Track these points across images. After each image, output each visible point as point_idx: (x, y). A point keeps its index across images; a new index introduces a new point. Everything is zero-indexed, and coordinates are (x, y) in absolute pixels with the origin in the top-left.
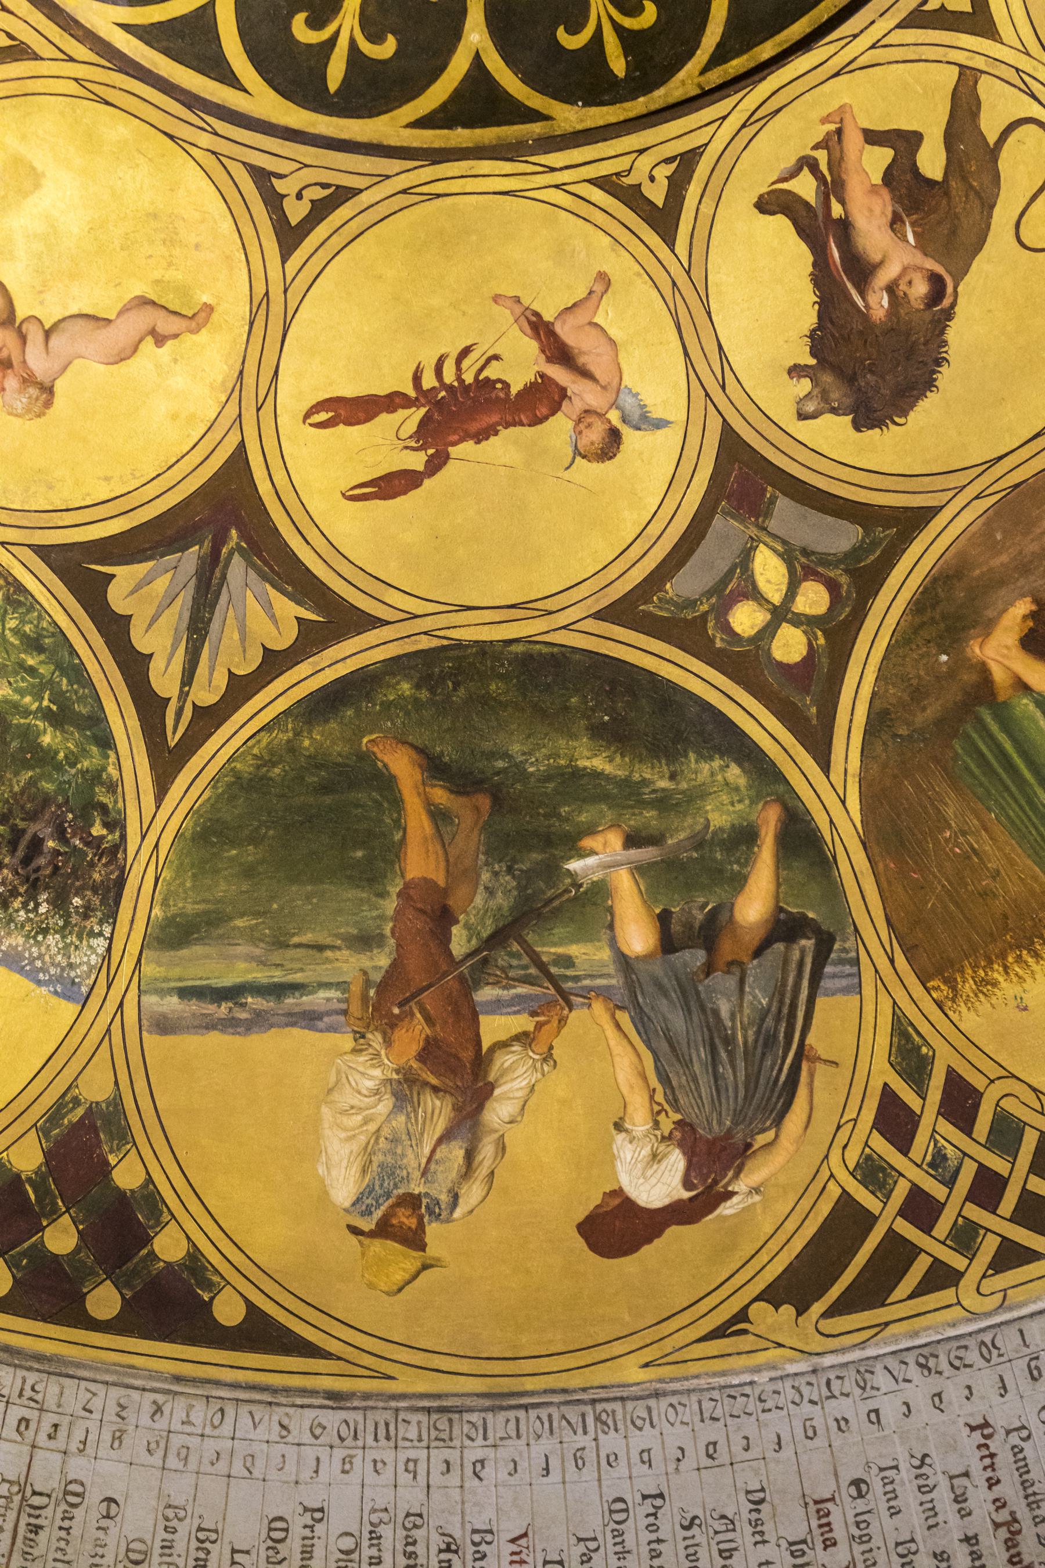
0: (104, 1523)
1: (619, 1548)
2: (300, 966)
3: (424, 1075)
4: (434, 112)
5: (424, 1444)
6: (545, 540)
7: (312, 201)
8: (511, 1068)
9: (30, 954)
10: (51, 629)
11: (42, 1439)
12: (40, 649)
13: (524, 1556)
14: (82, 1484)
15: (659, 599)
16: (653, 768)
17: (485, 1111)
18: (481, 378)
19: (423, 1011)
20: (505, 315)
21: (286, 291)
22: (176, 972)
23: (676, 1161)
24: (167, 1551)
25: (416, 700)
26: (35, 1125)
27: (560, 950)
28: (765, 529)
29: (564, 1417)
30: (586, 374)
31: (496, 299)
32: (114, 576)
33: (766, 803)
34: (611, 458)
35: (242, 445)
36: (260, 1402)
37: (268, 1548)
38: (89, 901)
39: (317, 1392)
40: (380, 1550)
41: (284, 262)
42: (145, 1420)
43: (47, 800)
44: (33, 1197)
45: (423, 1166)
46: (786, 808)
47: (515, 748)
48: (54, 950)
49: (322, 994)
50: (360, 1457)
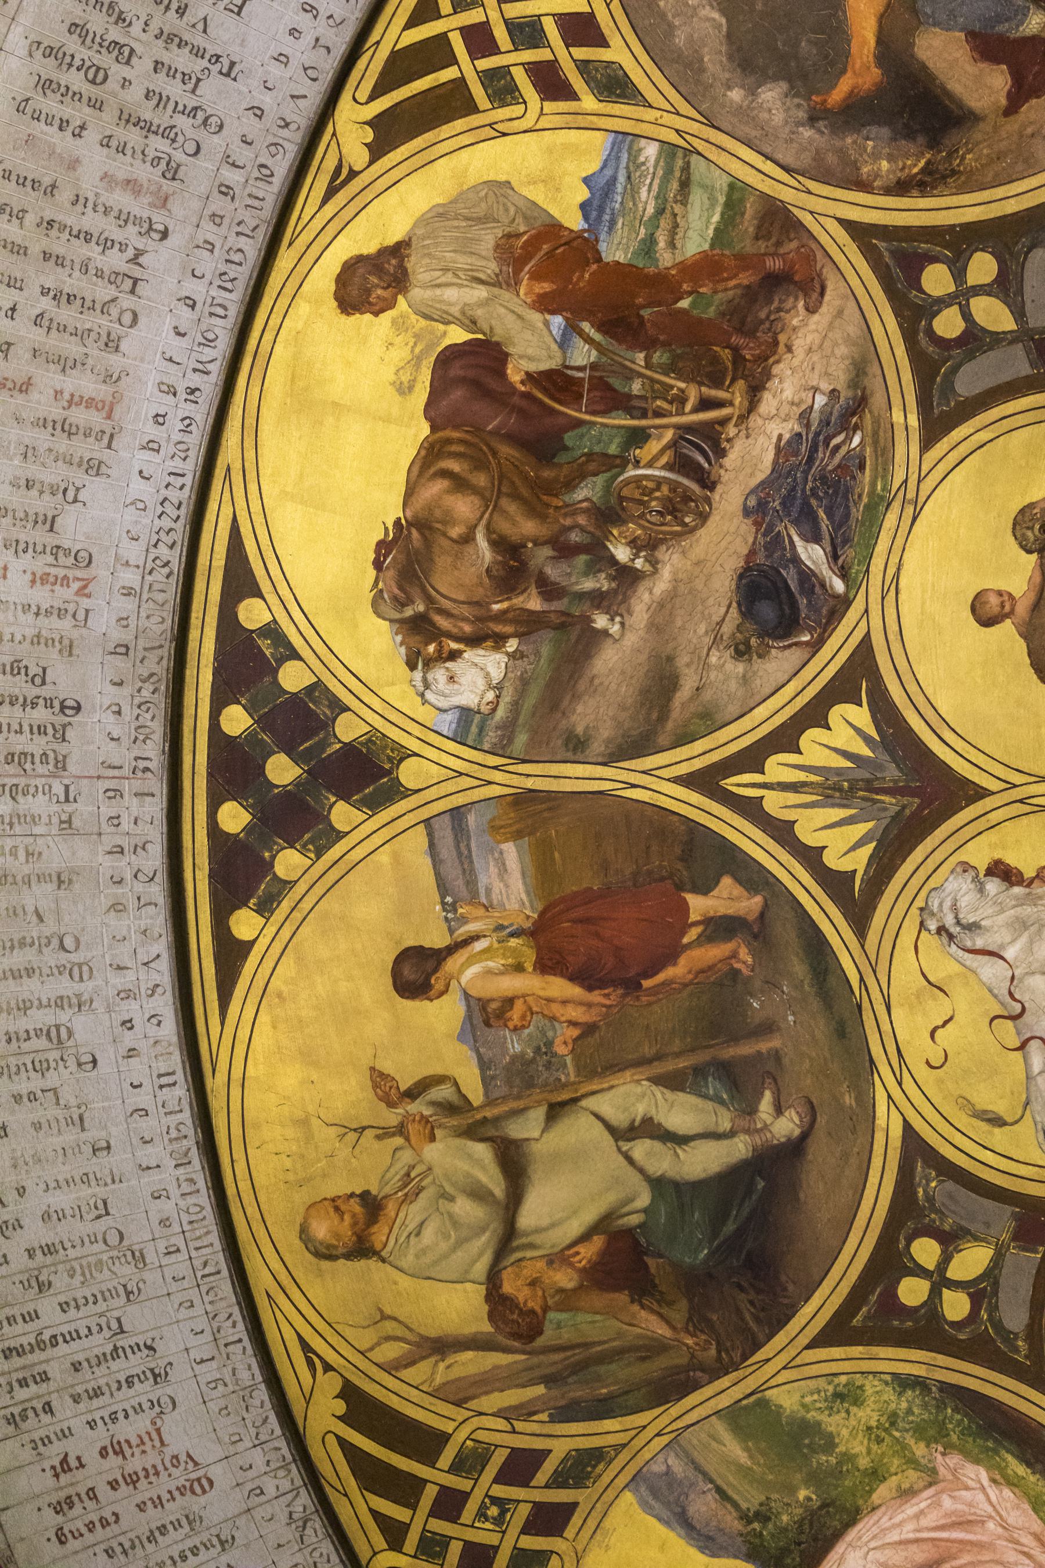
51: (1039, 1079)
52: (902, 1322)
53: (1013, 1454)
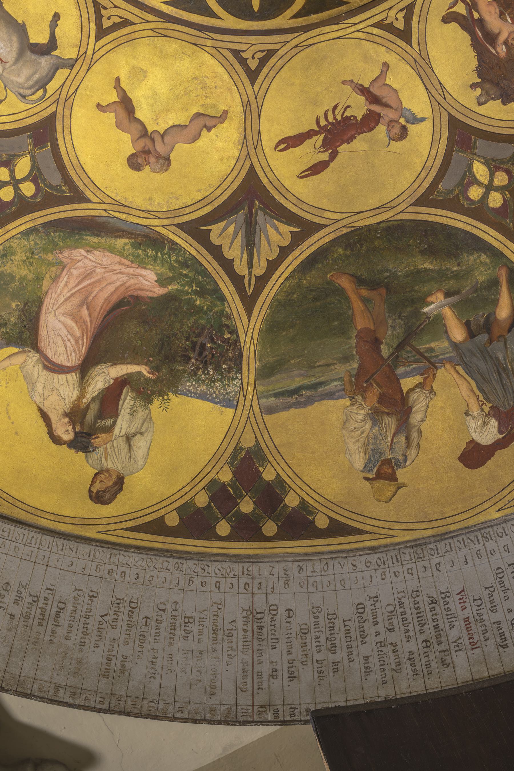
0: (288, 620)
1: (503, 589)
2: (321, 374)
3: (382, 409)
4: (300, 10)
5: (413, 561)
6: (386, 177)
7: (259, 59)
8: (418, 399)
9: (210, 392)
10: (190, 257)
11: (256, 590)
12: (187, 266)
13: (464, 600)
14: (276, 605)
15: (437, 192)
16: (450, 263)
17: (410, 419)
18: (344, 116)
19: (376, 382)
20: (348, 89)
21: (256, 98)
22: (271, 387)
23: (494, 423)
24: (317, 626)
25: (346, 255)
26: (227, 461)
27: (427, 346)
28: (475, 154)
29: (469, 538)
30: (387, 106)
31: (344, 82)
32: (211, 230)
33: (500, 267)
34: (405, 138)
35: (252, 165)
36: (342, 557)
37: (358, 617)
38: (229, 365)
39: (365, 549)
40: (404, 609)
41: (253, 86)
42: (296, 574)
43: (203, 328)
44: (232, 492)
45: (389, 446)
46: (508, 268)
47: (391, 266)
48: (219, 388)
49: (333, 384)
50: (388, 572)
51: (4, 74)
52: (10, 209)
53: (89, 235)
